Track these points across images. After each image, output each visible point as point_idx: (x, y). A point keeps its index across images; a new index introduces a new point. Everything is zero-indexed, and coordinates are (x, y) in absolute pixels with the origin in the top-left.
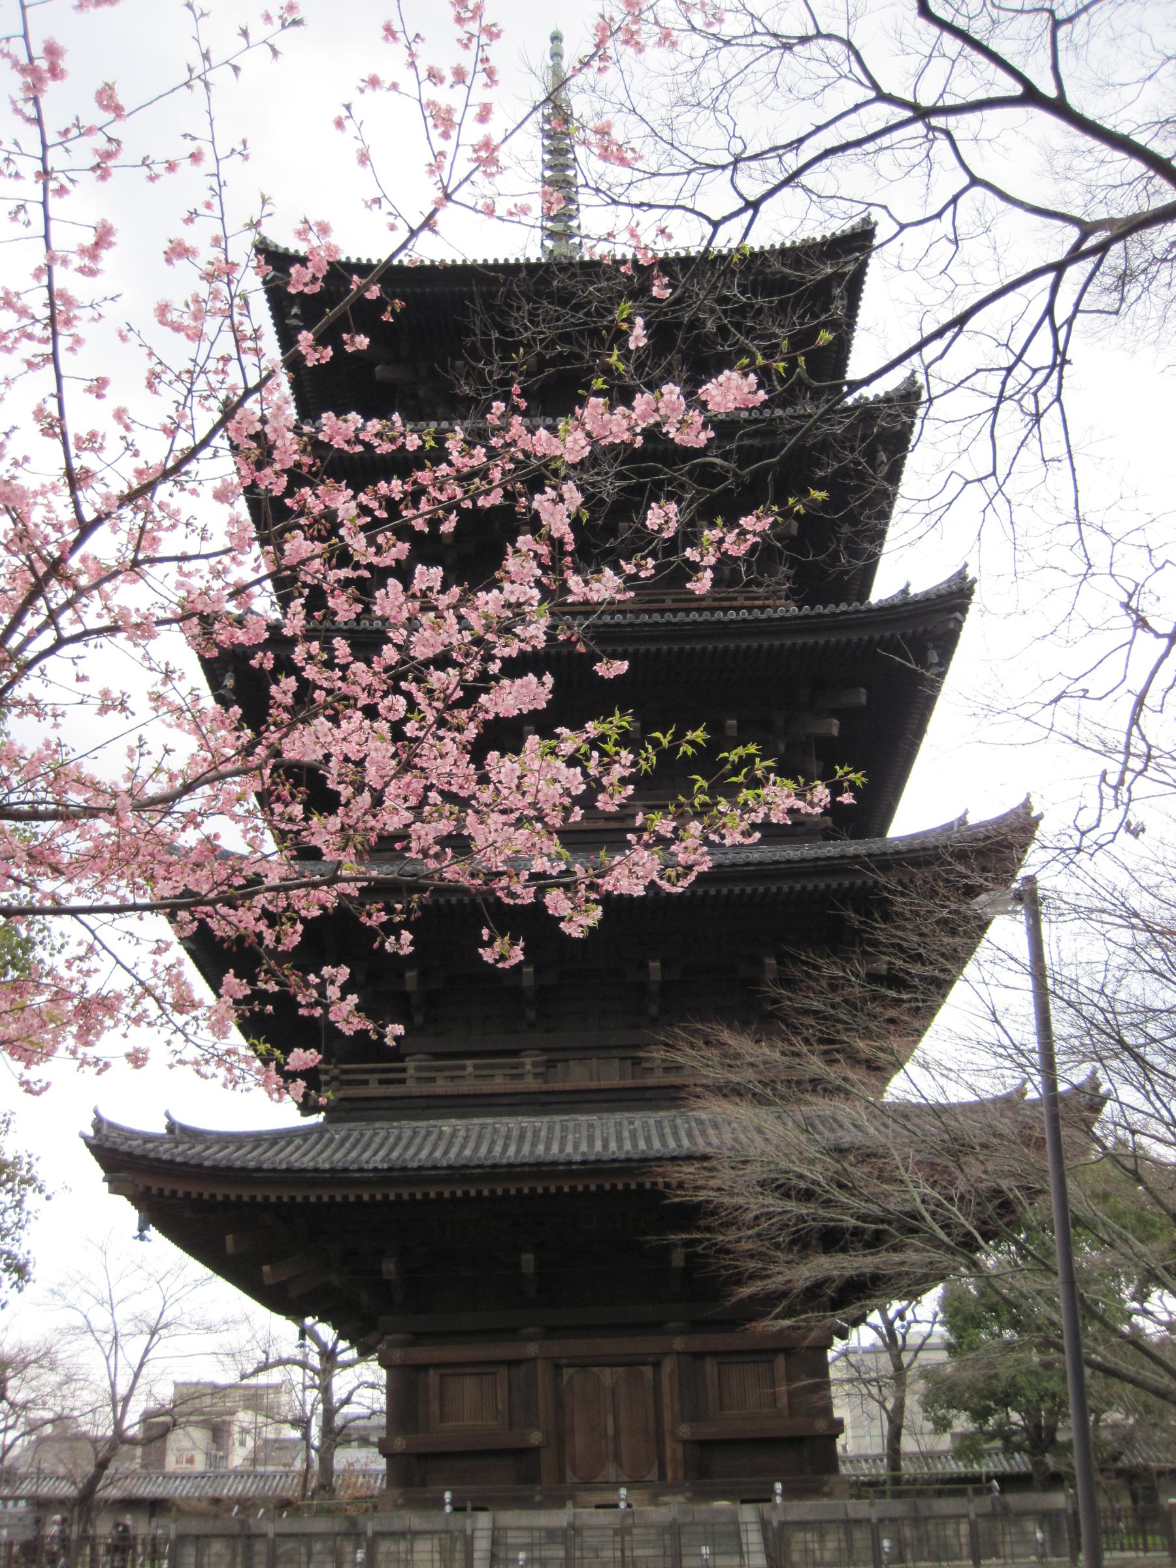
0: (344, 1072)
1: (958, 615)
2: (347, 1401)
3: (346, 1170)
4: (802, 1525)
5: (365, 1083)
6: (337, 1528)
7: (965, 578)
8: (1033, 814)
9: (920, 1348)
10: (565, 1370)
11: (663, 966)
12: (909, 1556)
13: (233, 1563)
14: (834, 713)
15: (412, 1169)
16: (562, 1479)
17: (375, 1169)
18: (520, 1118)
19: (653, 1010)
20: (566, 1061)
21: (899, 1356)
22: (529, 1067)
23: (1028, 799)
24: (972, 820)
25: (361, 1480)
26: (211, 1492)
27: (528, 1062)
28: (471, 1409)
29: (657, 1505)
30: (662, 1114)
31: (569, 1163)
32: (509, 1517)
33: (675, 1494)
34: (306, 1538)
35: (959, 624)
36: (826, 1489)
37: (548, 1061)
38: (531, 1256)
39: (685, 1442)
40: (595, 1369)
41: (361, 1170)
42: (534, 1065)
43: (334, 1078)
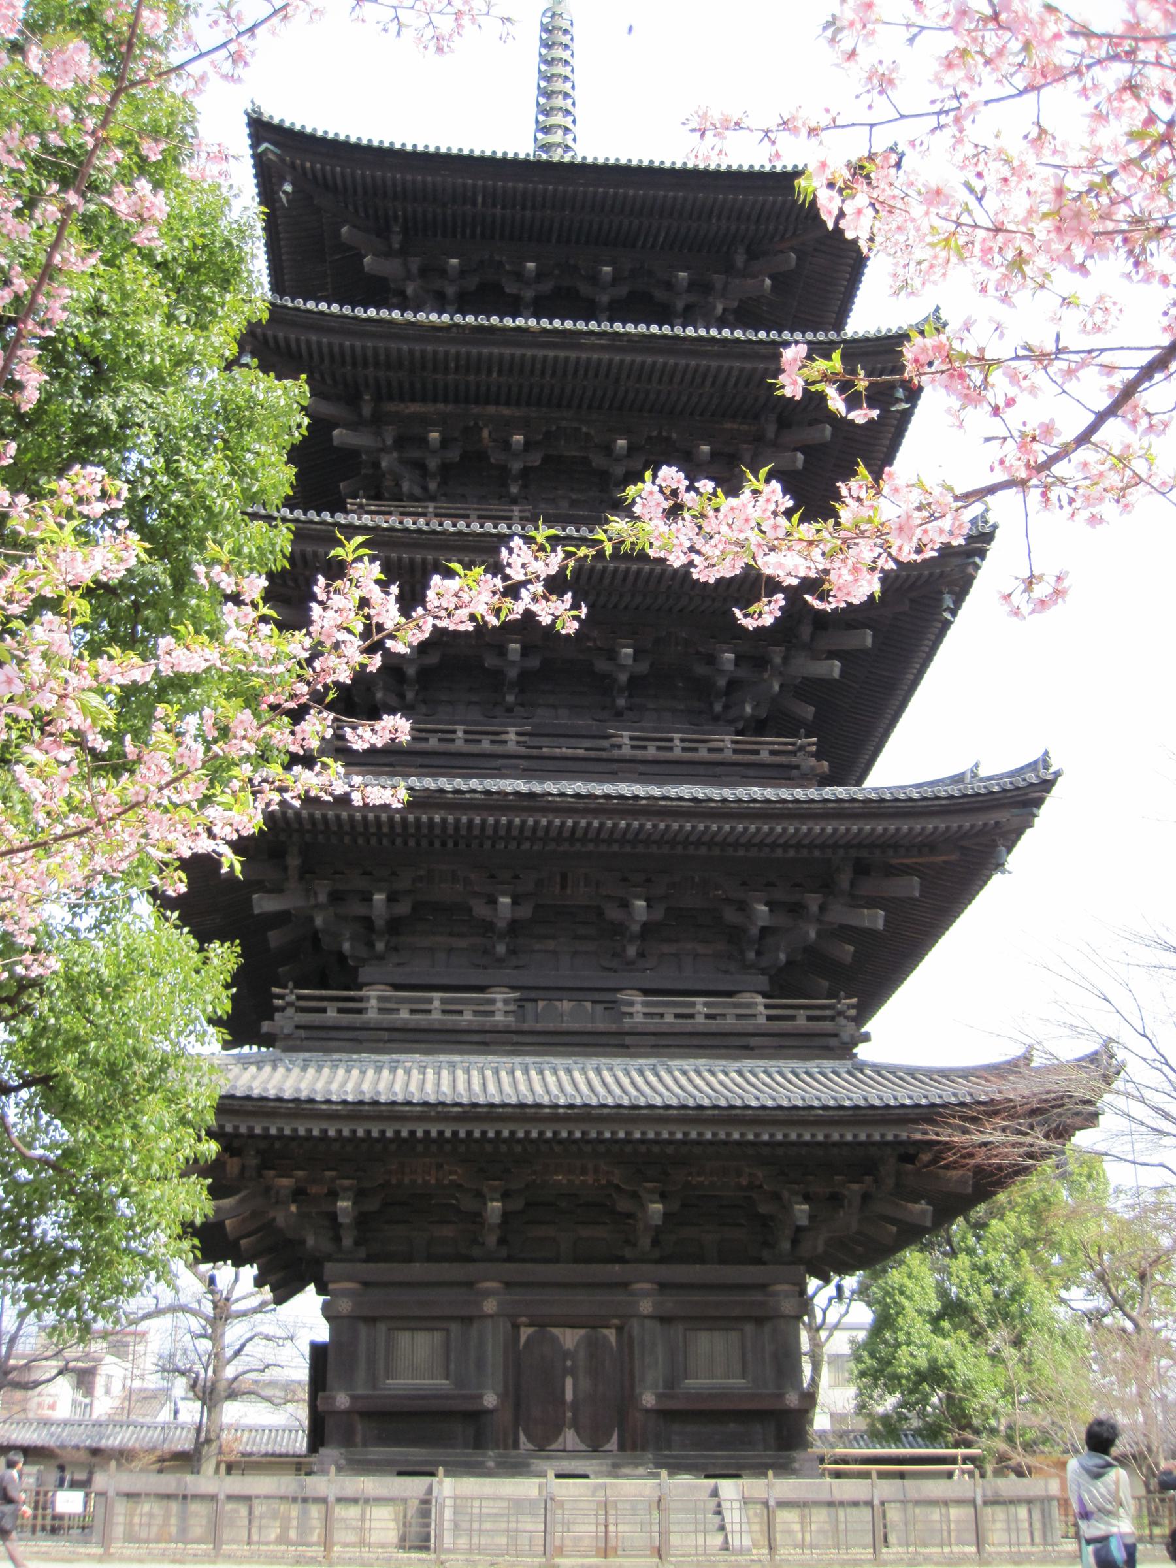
0: (299, 998)
1: (977, 560)
2: (237, 1353)
3: (311, 1101)
4: (783, 1504)
5: (324, 1010)
6: (282, 1491)
7: (986, 522)
8: (1052, 770)
9: (836, 1326)
10: (523, 1329)
11: (649, 906)
12: (892, 1538)
13: (166, 1523)
14: (832, 655)
15: (386, 1104)
16: (516, 1445)
17: (345, 1102)
18: (490, 1058)
19: (632, 951)
20: (536, 1000)
21: (818, 1329)
22: (500, 1005)
23: (1046, 753)
24: (983, 772)
25: (246, 1435)
26: (88, 1442)
27: (499, 996)
28: (415, 1365)
29: (617, 1477)
30: (642, 1061)
31: (557, 1106)
32: (470, 1485)
33: (636, 1466)
34: (247, 1499)
35: (978, 567)
36: (796, 1465)
37: (516, 1000)
38: (497, 1204)
39: (647, 1411)
40: (556, 1331)
41: (328, 1102)
42: (506, 1002)
43: (290, 1004)
